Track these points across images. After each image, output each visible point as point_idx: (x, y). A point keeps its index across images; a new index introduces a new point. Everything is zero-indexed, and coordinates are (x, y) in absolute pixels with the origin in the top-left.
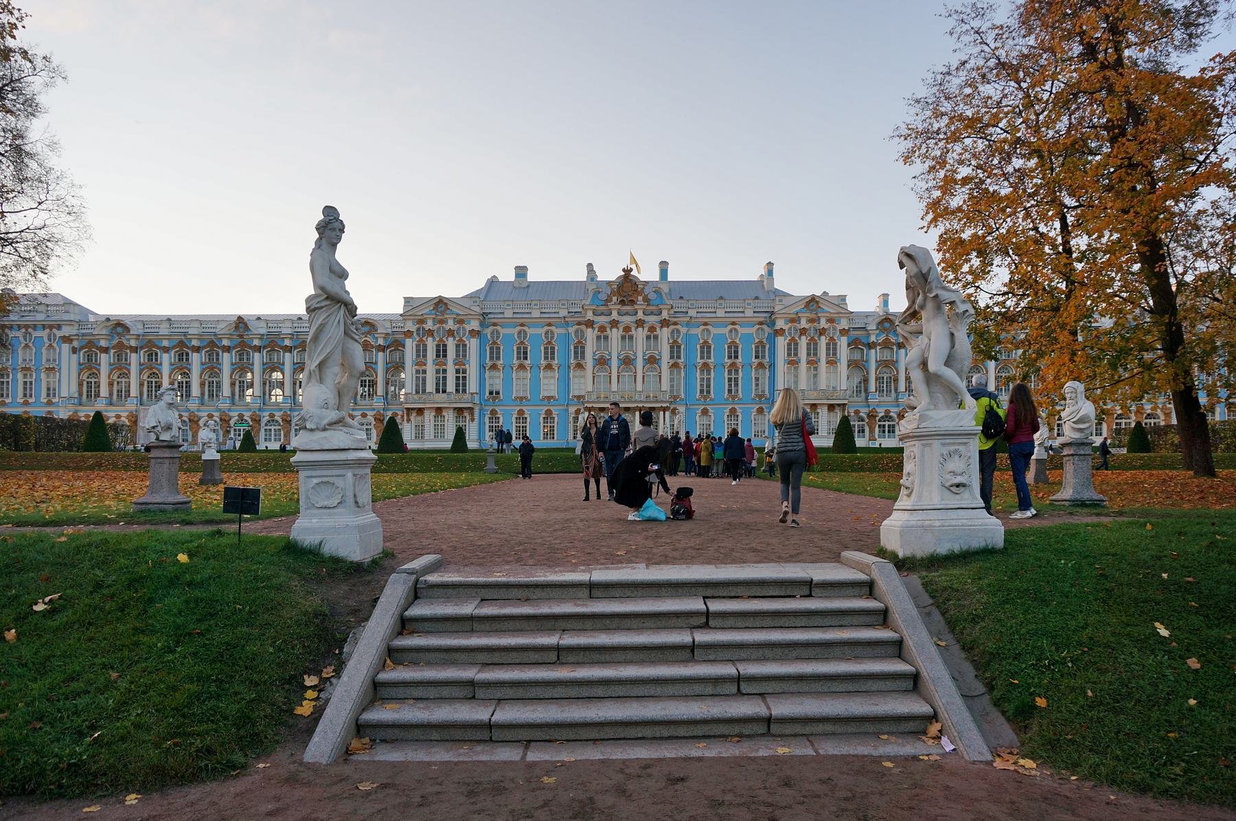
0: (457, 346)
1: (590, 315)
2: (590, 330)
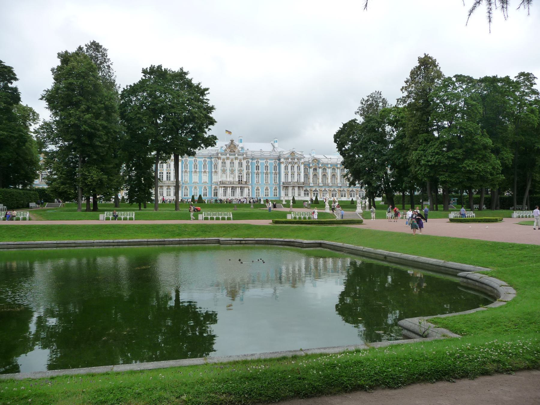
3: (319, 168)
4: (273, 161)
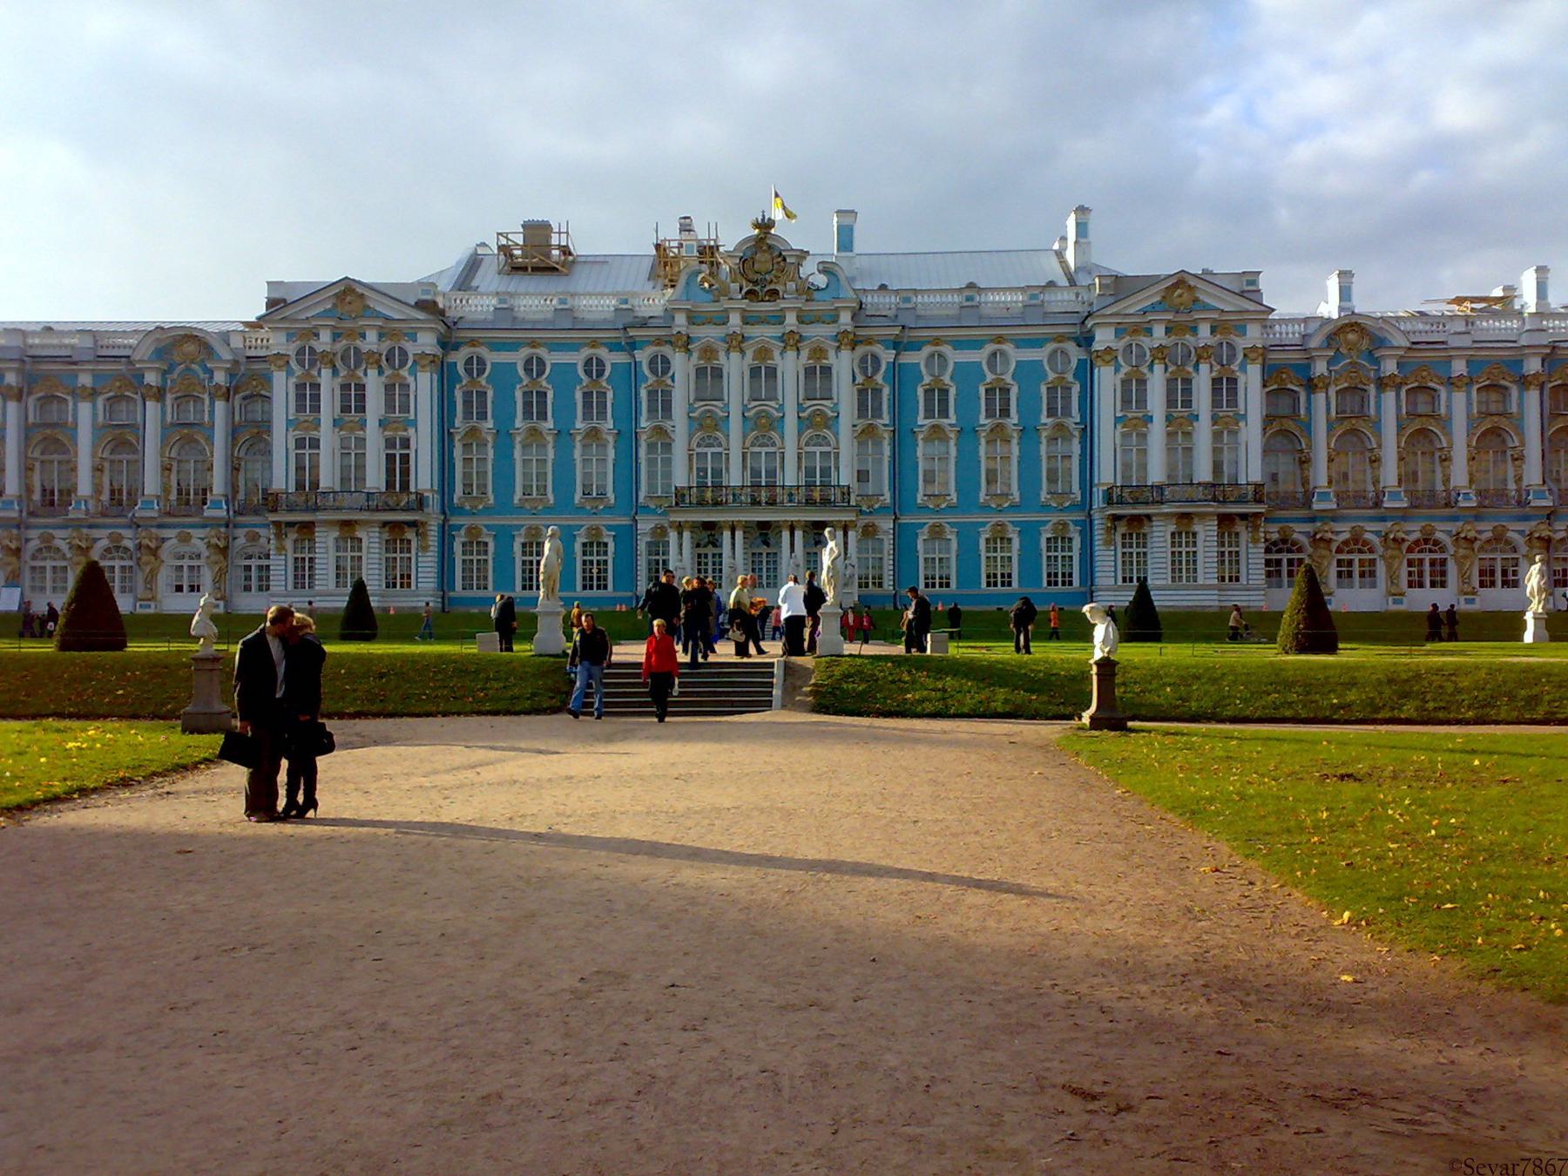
0: (389, 388)
3: (1382, 384)
4: (1040, 355)
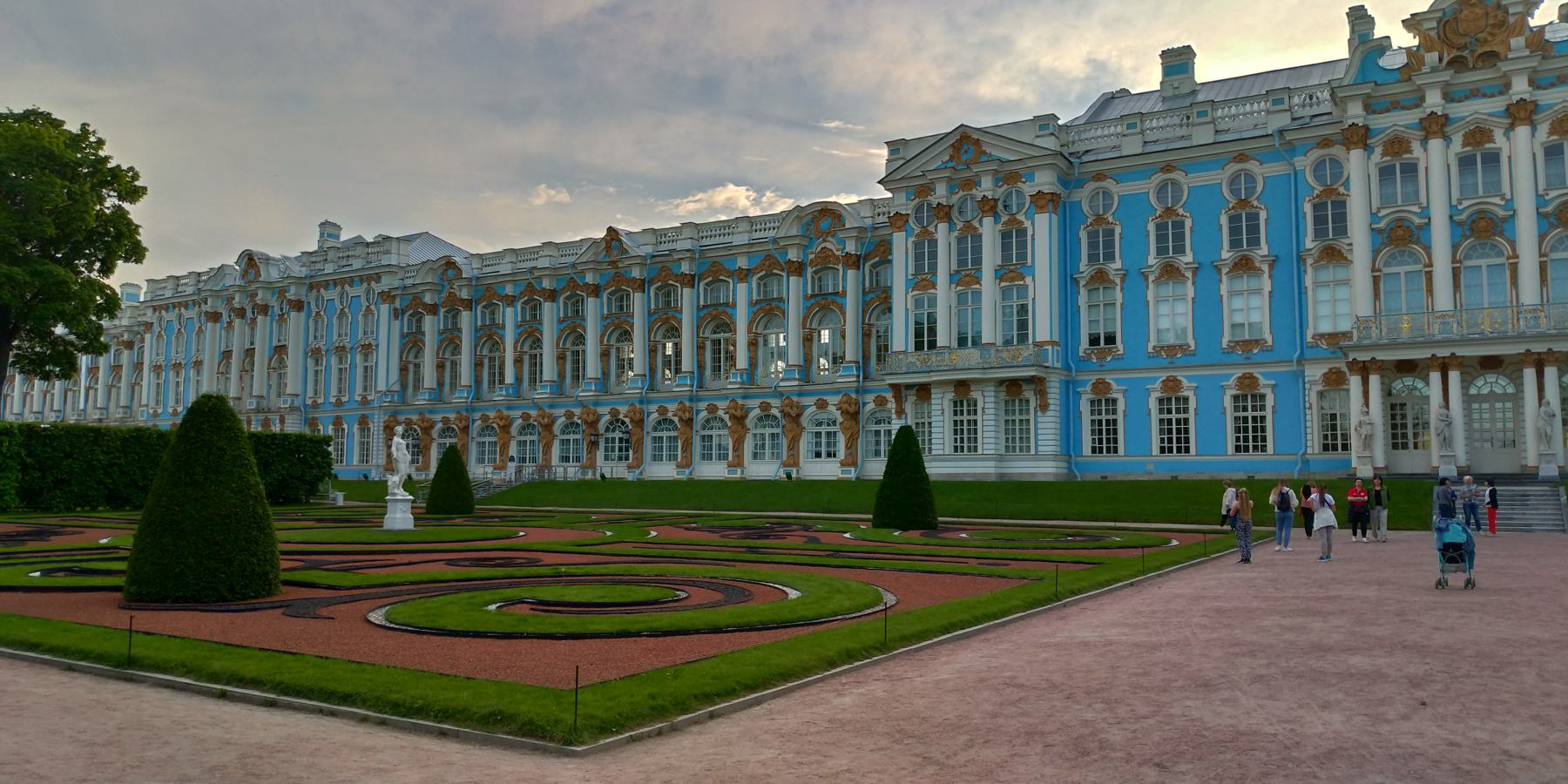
0: (1005, 236)
1: (1355, 113)
2: (1356, 155)
